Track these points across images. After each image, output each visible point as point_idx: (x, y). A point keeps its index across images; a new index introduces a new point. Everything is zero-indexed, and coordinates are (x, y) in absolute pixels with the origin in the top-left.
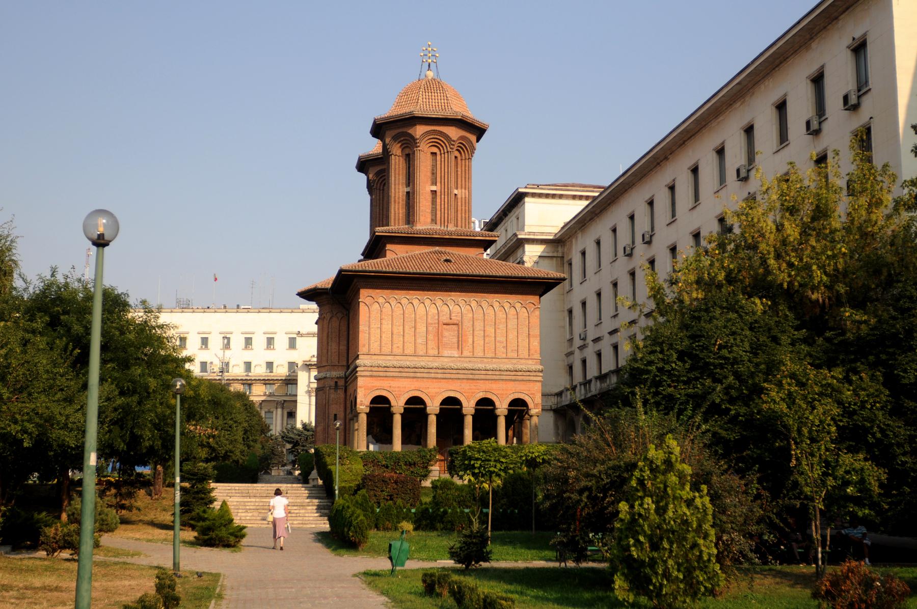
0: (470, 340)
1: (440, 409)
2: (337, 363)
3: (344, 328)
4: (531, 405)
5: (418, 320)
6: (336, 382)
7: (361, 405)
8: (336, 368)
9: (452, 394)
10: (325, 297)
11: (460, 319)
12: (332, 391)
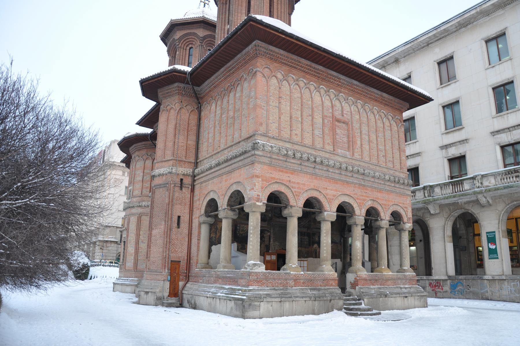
0: (359, 142)
1: (337, 216)
2: (184, 160)
3: (194, 122)
4: (405, 219)
5: (315, 109)
6: (182, 180)
7: (258, 201)
8: (182, 163)
9: (347, 199)
10: (176, 84)
11: (349, 118)
12: (177, 189)
